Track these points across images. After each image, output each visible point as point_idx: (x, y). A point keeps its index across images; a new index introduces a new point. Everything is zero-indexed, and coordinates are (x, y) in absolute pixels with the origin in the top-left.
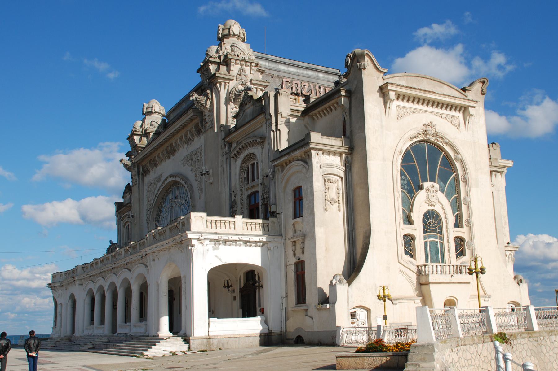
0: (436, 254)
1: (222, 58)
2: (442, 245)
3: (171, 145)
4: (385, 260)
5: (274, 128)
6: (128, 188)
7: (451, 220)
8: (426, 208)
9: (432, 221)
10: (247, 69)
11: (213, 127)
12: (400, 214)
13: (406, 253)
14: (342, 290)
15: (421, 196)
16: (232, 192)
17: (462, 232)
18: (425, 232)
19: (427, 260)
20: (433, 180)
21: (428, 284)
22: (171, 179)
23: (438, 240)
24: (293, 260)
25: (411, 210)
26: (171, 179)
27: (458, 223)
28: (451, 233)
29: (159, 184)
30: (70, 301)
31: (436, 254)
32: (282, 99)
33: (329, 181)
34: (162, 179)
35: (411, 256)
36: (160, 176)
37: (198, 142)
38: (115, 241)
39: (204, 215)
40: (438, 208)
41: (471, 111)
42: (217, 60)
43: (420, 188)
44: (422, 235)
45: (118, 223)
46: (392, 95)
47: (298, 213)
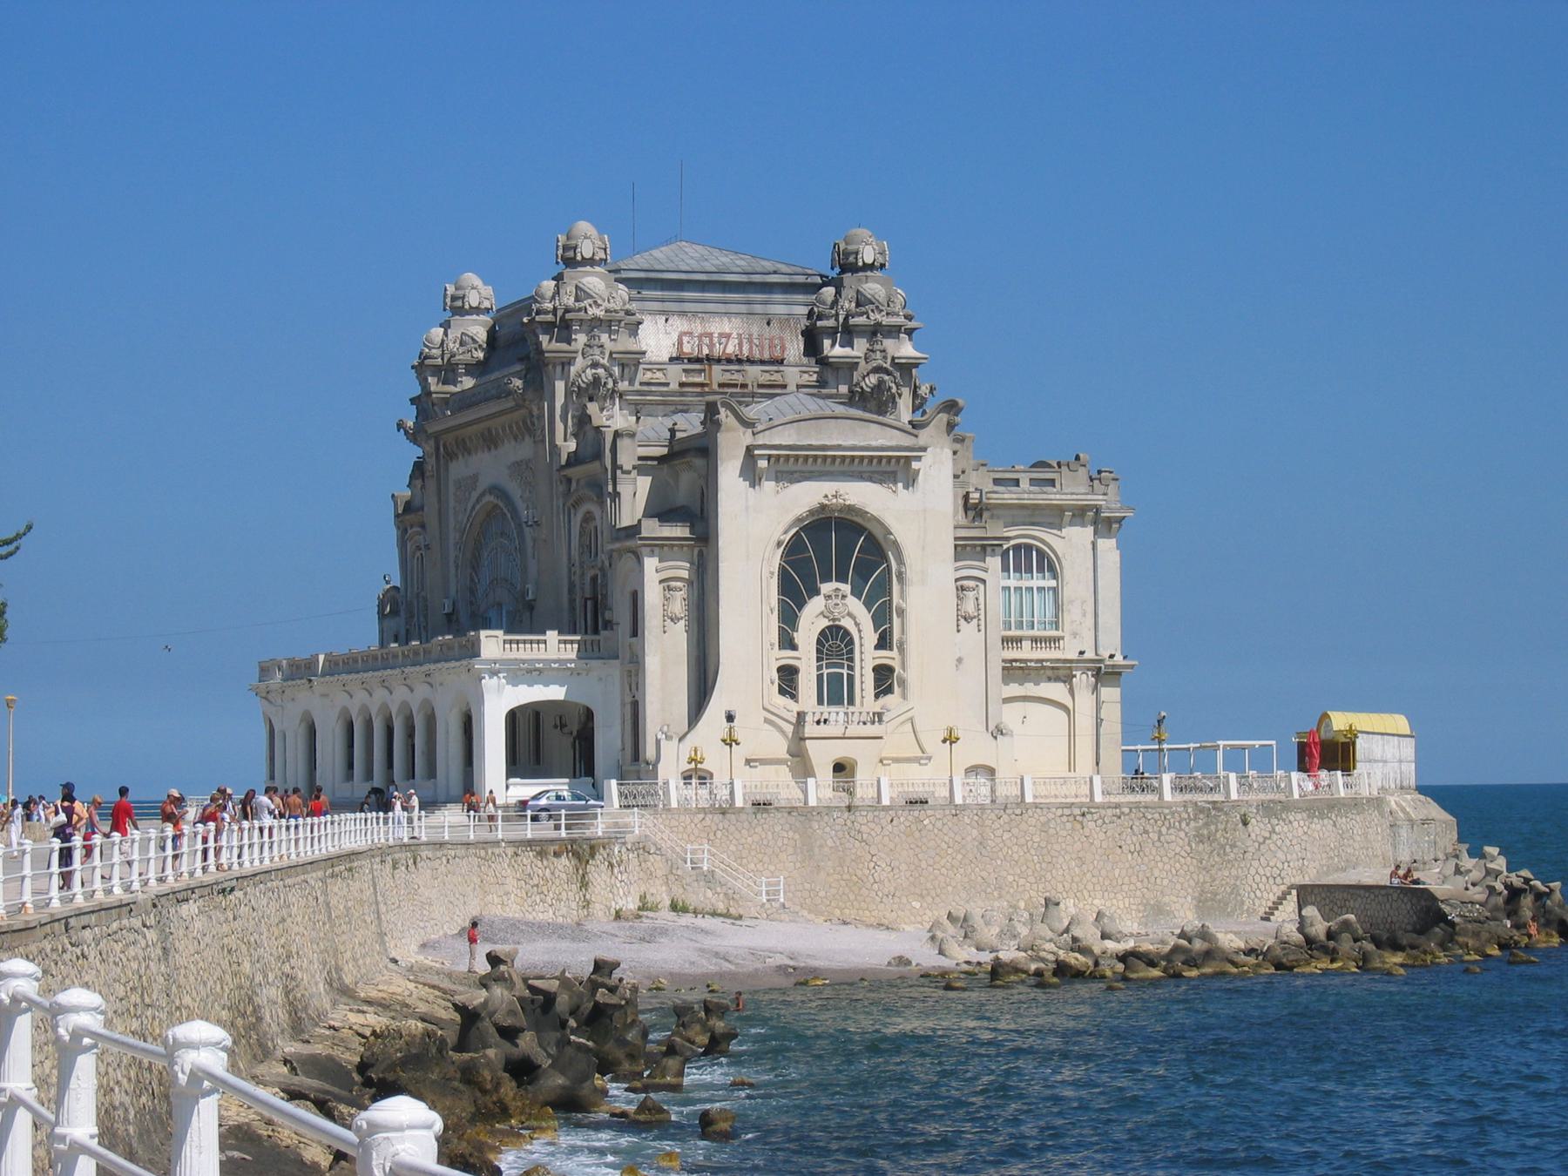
1: (559, 313)
2: (851, 678)
3: (489, 430)
5: (610, 489)
6: (419, 469)
7: (871, 637)
8: (826, 623)
9: (835, 642)
11: (543, 441)
12: (774, 636)
13: (782, 692)
14: (669, 748)
15: (815, 605)
16: (571, 565)
17: (889, 657)
18: (819, 659)
19: (820, 702)
20: (842, 578)
21: (804, 739)
22: (489, 498)
23: (845, 672)
24: (629, 699)
25: (795, 629)
26: (489, 498)
27: (884, 642)
28: (867, 656)
29: (475, 495)
30: (303, 725)
31: (836, 691)
32: (623, 444)
33: (670, 589)
34: (480, 490)
35: (794, 697)
36: (475, 478)
38: (396, 581)
39: (500, 633)
40: (847, 623)
41: (915, 465)
42: (550, 317)
43: (815, 592)
44: (814, 663)
45: (402, 544)
46: (763, 464)
47: (635, 633)
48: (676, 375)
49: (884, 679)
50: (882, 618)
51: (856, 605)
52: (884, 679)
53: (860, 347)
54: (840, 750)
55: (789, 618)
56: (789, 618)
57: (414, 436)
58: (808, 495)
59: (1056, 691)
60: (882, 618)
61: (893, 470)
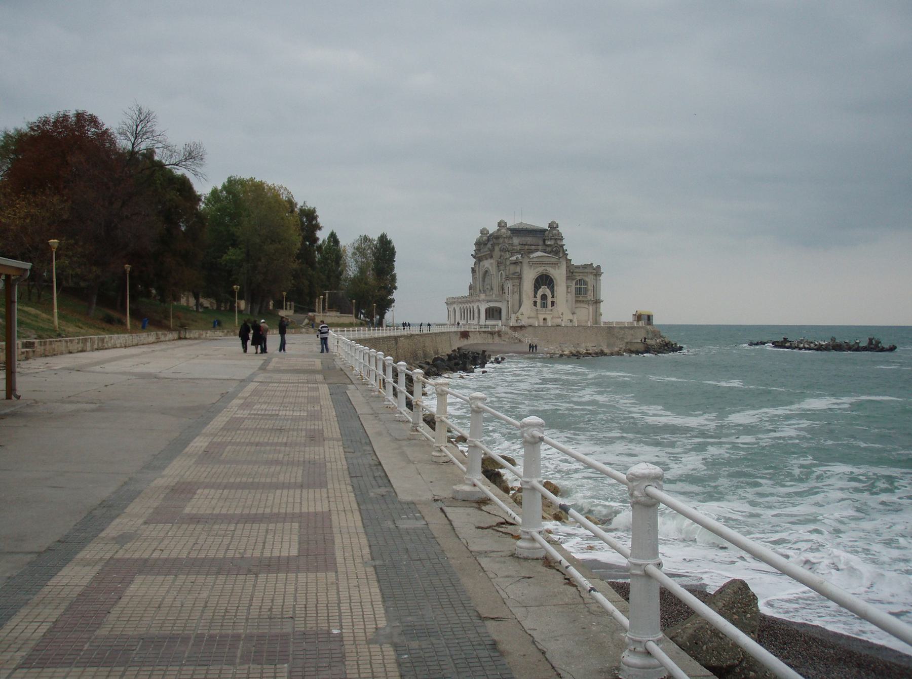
0: (544, 306)
4: (527, 307)
9: (544, 297)
10: (506, 240)
14: (513, 316)
15: (541, 290)
27: (553, 297)
31: (544, 306)
37: (492, 261)
48: (519, 247)
49: (553, 303)
50: (553, 292)
51: (548, 290)
52: (553, 303)
53: (552, 242)
54: (545, 316)
55: (536, 293)
56: (536, 293)
57: (474, 257)
58: (540, 270)
59: (586, 306)
60: (553, 292)
61: (555, 265)
